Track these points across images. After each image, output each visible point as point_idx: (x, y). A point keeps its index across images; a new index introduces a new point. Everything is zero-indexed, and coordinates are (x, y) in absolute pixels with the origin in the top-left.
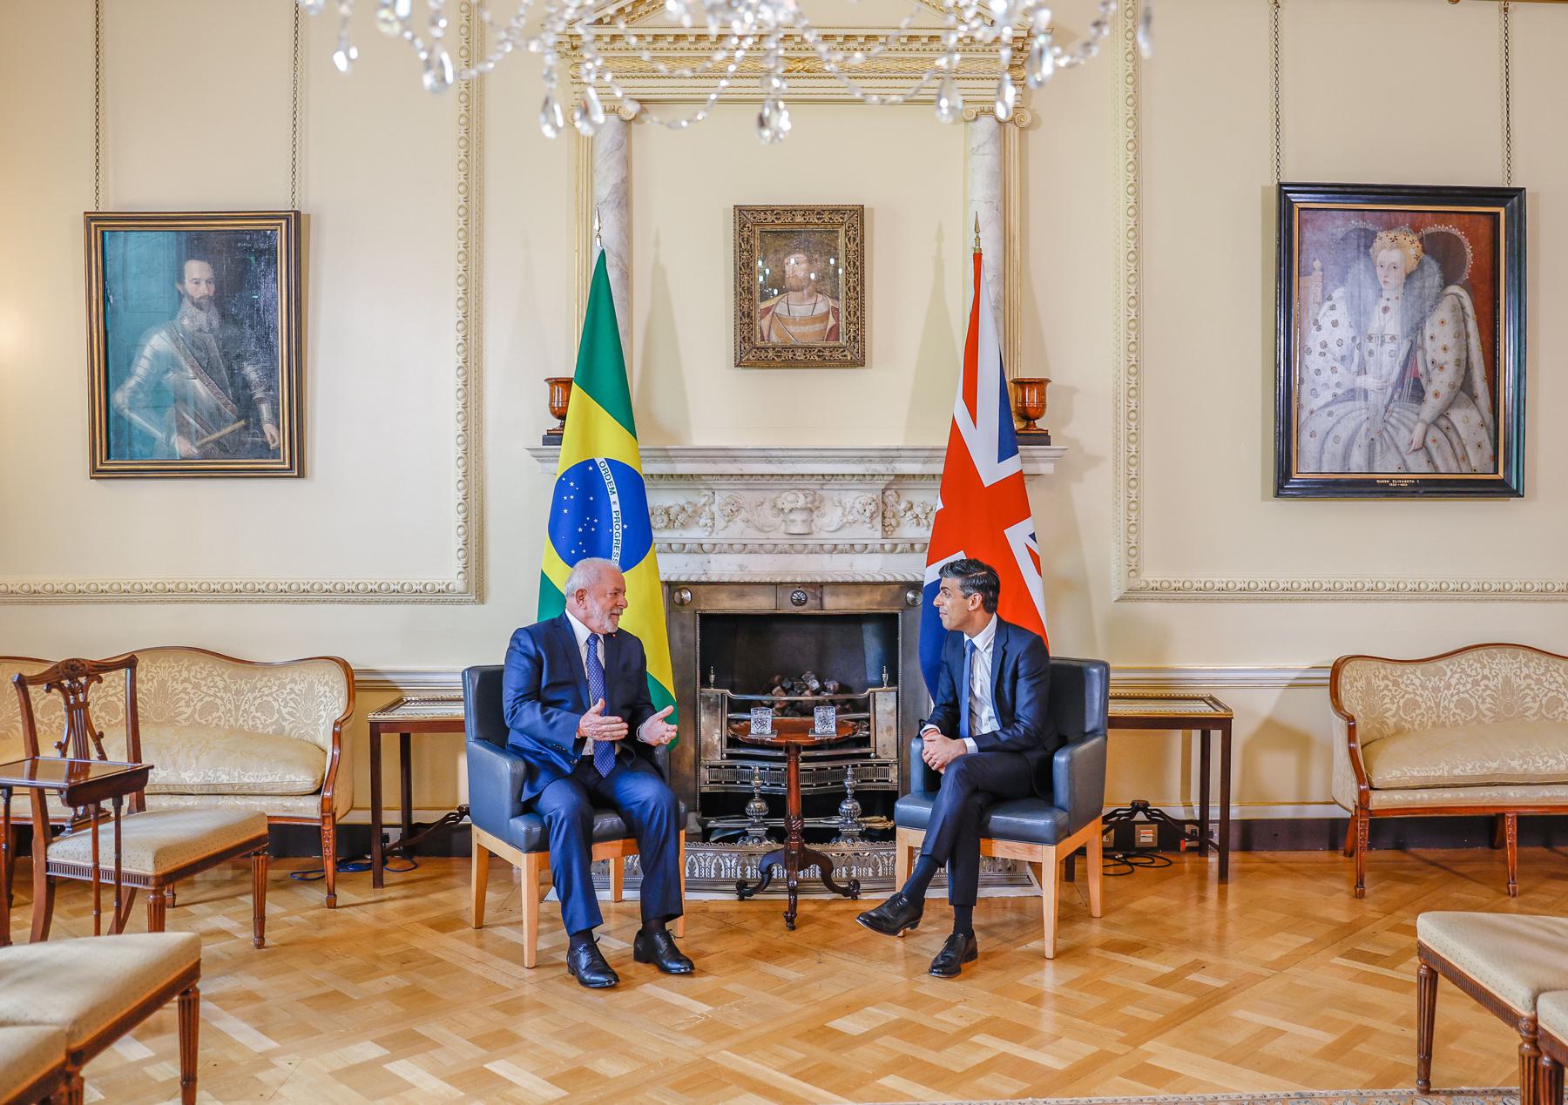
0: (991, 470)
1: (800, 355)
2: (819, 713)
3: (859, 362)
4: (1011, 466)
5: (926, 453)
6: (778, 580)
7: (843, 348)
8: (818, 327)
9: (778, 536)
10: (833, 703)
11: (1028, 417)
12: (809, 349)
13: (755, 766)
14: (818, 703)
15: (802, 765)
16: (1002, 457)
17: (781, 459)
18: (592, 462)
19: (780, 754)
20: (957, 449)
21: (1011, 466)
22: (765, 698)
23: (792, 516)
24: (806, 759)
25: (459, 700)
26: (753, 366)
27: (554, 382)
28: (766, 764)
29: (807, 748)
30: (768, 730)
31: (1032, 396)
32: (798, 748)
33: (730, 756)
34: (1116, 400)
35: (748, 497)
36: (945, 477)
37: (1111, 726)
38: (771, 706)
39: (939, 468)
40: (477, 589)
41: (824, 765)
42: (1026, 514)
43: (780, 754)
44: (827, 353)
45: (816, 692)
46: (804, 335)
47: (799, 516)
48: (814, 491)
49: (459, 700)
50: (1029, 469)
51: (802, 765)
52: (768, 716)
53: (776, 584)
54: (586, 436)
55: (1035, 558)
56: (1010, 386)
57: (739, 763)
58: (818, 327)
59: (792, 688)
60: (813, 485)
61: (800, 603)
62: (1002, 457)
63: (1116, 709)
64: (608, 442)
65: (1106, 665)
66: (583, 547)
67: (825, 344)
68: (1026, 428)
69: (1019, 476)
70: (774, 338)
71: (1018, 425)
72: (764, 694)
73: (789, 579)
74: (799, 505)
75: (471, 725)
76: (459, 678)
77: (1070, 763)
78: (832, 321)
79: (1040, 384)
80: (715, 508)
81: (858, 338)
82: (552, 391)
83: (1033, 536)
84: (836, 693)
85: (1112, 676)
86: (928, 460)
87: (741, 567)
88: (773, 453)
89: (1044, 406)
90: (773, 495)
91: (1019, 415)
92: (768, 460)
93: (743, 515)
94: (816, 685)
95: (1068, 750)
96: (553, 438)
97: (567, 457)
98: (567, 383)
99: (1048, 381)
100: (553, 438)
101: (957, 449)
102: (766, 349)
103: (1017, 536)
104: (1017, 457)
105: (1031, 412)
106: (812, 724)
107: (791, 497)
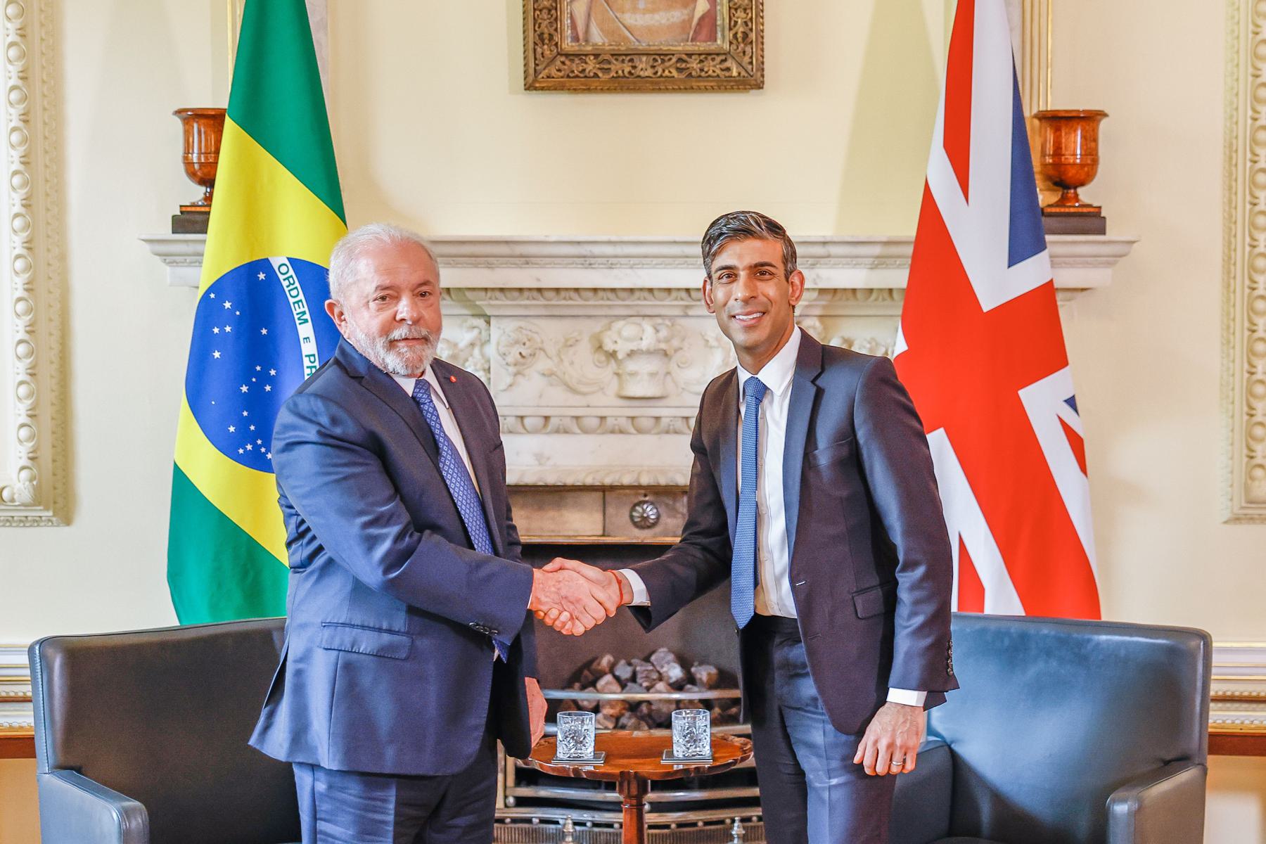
0: (995, 281)
1: (644, 67)
2: (680, 721)
3: (751, 81)
4: (1032, 274)
5: (877, 250)
6: (608, 481)
7: (723, 59)
8: (677, 15)
9: (606, 402)
10: (707, 704)
11: (1064, 182)
12: (660, 56)
13: (566, 818)
14: (679, 704)
15: (651, 818)
16: (1016, 256)
17: (610, 263)
18: (264, 264)
19: (612, 796)
20: (933, 244)
21: (1032, 274)
22: (586, 696)
23: (631, 366)
24: (658, 807)
25: (25, 700)
26: (559, 88)
27: (192, 117)
28: (586, 816)
29: (660, 785)
30: (588, 750)
31: (1075, 142)
32: (643, 784)
33: (521, 802)
34: (1231, 150)
35: (550, 331)
36: (912, 294)
37: (1211, 752)
38: (596, 710)
39: (899, 278)
40: (55, 495)
41: (691, 816)
42: (1055, 359)
43: (612, 796)
44: (694, 64)
45: (678, 686)
46: (650, 30)
47: (644, 366)
48: (671, 317)
49: (25, 700)
50: (1064, 278)
51: (651, 818)
52: (589, 726)
53: (604, 490)
54: (253, 214)
55: (1076, 443)
56: (1032, 125)
57: (536, 814)
58: (677, 15)
59: (633, 678)
60: (669, 307)
61: (644, 524)
62: (1016, 256)
63: (1221, 718)
64: (293, 226)
65: (1204, 637)
66: (249, 420)
67: (690, 47)
68: (1062, 202)
69: (1047, 293)
70: (597, 37)
71: (1045, 197)
72: (583, 688)
73: (627, 480)
74: (644, 345)
75: (43, 746)
76: (24, 659)
77: (1137, 814)
78: (702, 6)
79: (1090, 119)
80: (491, 350)
81: (749, 37)
82: (187, 134)
83: (1071, 402)
84: (712, 687)
85: (1216, 659)
86: (879, 262)
87: (540, 457)
88: (597, 250)
89: (1095, 162)
90: (596, 326)
91: (1048, 178)
92: (587, 261)
93: (542, 364)
94: (676, 672)
95: (1134, 792)
96: (191, 221)
97: (218, 254)
98: (214, 119)
99: (1105, 115)
100: (191, 221)
101: (933, 244)
102: (581, 56)
103: (1041, 401)
104: (1044, 255)
105: (1071, 172)
106: (669, 743)
107: (627, 329)
